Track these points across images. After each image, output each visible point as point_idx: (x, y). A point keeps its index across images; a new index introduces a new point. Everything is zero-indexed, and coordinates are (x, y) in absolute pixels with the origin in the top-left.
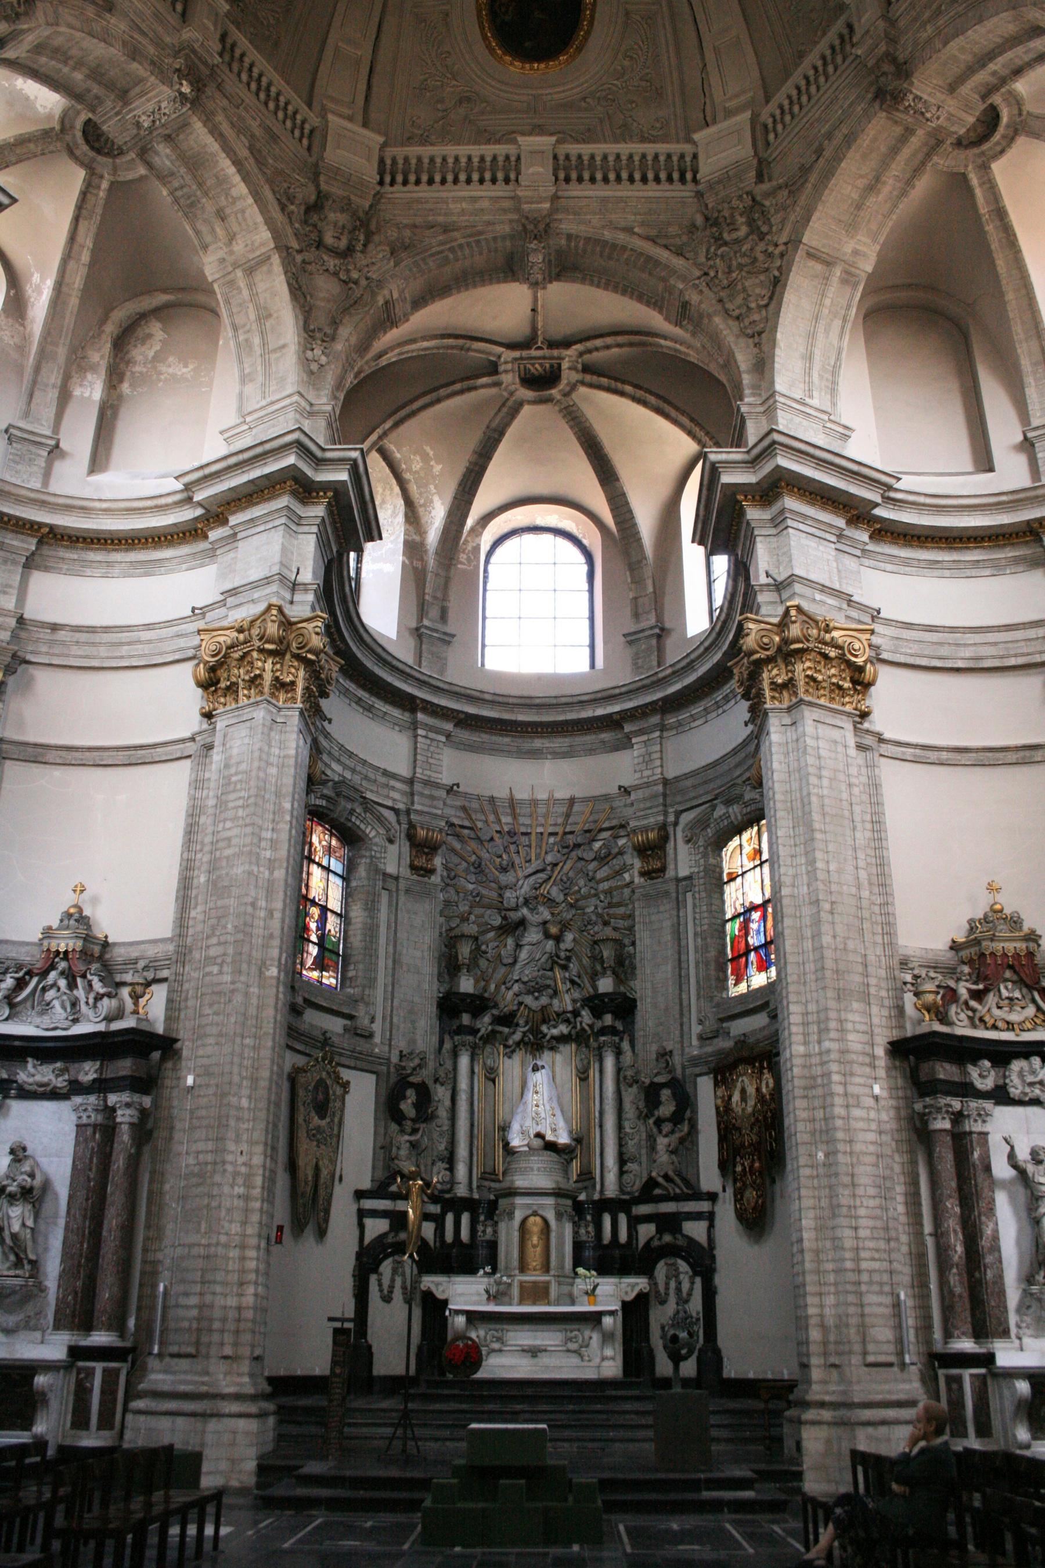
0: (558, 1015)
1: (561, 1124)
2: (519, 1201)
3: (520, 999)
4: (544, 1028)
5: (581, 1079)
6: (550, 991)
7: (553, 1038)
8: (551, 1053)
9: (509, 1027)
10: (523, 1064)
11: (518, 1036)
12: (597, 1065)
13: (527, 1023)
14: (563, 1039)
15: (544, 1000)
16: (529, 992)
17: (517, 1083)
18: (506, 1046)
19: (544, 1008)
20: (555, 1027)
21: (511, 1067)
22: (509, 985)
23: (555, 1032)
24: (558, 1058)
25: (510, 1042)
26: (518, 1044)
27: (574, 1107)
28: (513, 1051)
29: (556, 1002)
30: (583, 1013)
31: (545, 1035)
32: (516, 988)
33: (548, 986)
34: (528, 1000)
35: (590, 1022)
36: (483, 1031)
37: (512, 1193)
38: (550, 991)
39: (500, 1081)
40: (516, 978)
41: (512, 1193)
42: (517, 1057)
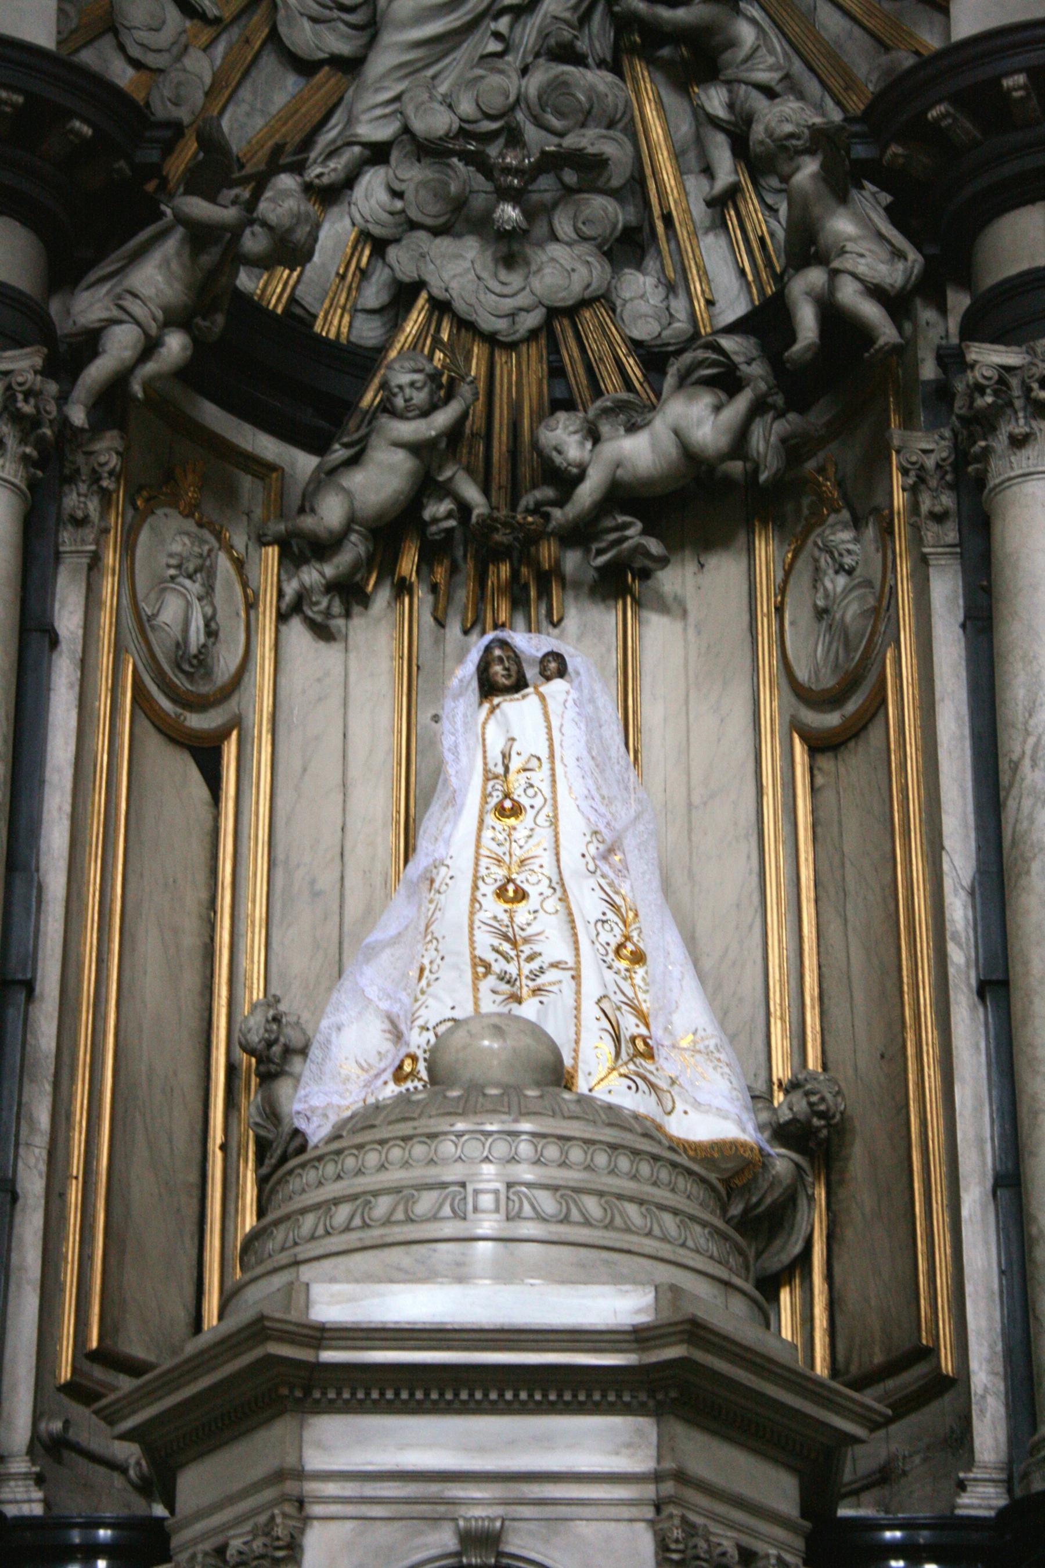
0: (654, 358)
1: (686, 1016)
2: (346, 1446)
3: (402, 260)
4: (565, 438)
5: (820, 746)
6: (604, 211)
7: (623, 496)
8: (607, 619)
9: (318, 446)
10: (416, 681)
11: (380, 477)
12: (946, 590)
13: (442, 388)
14: (695, 508)
15: (562, 268)
16: (457, 219)
17: (375, 801)
18: (300, 549)
19: (561, 317)
20: (634, 415)
21: (329, 696)
22: (325, 170)
23: (636, 453)
24: (660, 637)
25: (331, 512)
26: (390, 532)
27: (784, 947)
28: (350, 593)
29: (640, 289)
30: (842, 225)
31: (566, 481)
32: (372, 194)
33: (590, 168)
34: (458, 268)
35: (892, 274)
36: (120, 344)
37: (294, 1377)
38: (604, 211)
39: (254, 766)
40: (374, 130)
41: (294, 1377)
42: (376, 637)
